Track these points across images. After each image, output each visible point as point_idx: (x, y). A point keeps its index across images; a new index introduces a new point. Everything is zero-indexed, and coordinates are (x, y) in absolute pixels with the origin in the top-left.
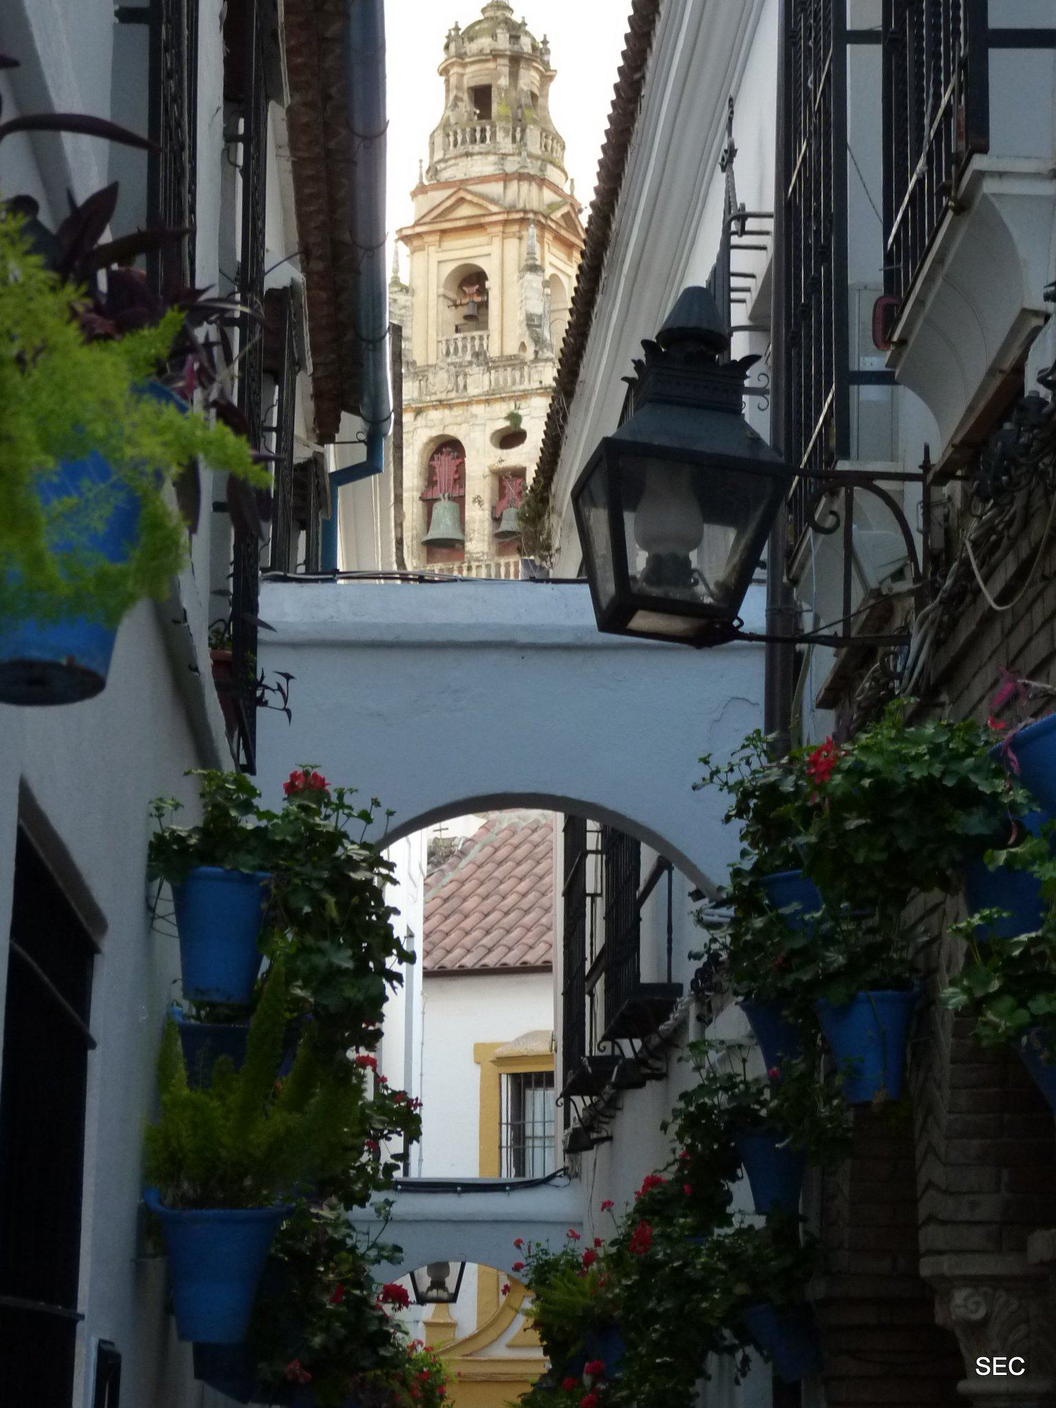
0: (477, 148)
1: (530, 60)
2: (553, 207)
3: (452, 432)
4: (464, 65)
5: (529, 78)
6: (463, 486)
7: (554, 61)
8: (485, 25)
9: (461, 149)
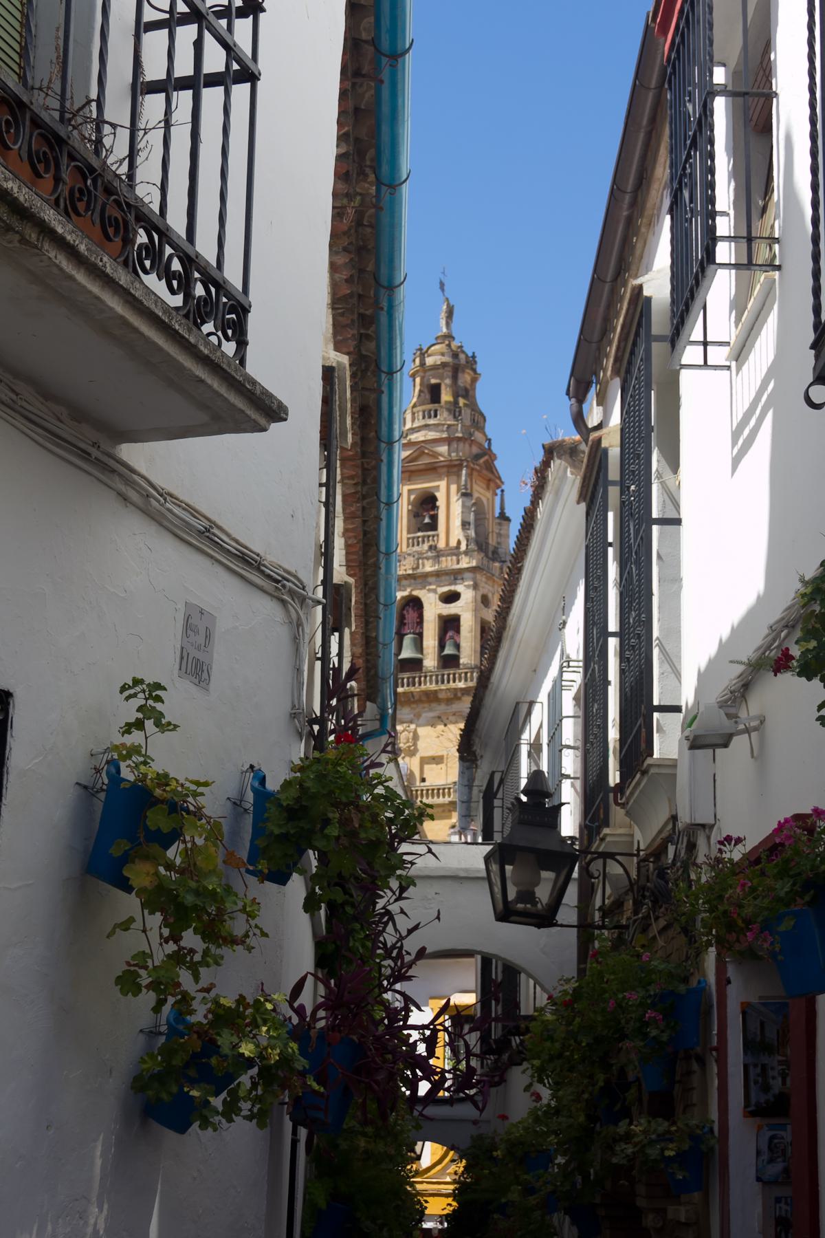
0: (432, 421)
1: (465, 367)
2: (477, 457)
3: (415, 593)
4: (425, 371)
5: (465, 378)
6: (422, 628)
7: (479, 369)
8: (437, 347)
9: (422, 423)
